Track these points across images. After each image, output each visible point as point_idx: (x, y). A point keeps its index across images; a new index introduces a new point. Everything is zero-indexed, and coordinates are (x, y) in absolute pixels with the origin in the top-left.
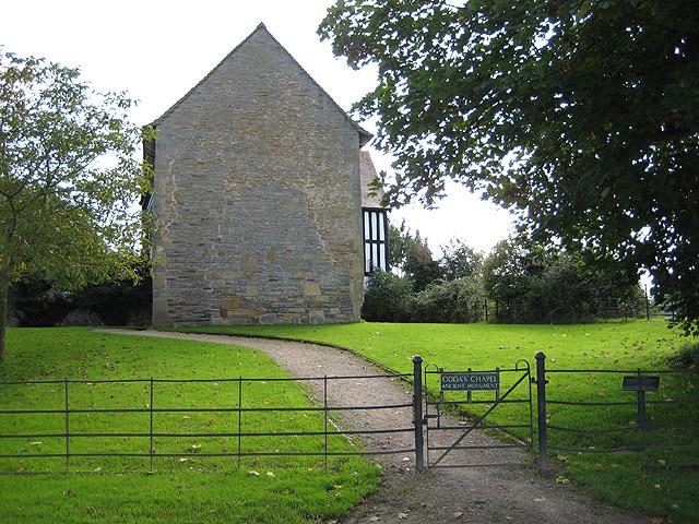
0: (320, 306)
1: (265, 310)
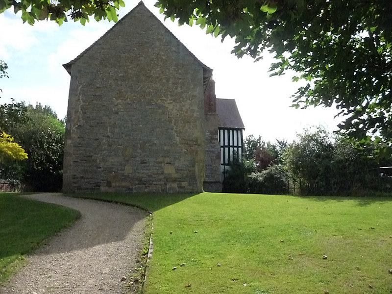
0: (174, 181)
1: (137, 182)
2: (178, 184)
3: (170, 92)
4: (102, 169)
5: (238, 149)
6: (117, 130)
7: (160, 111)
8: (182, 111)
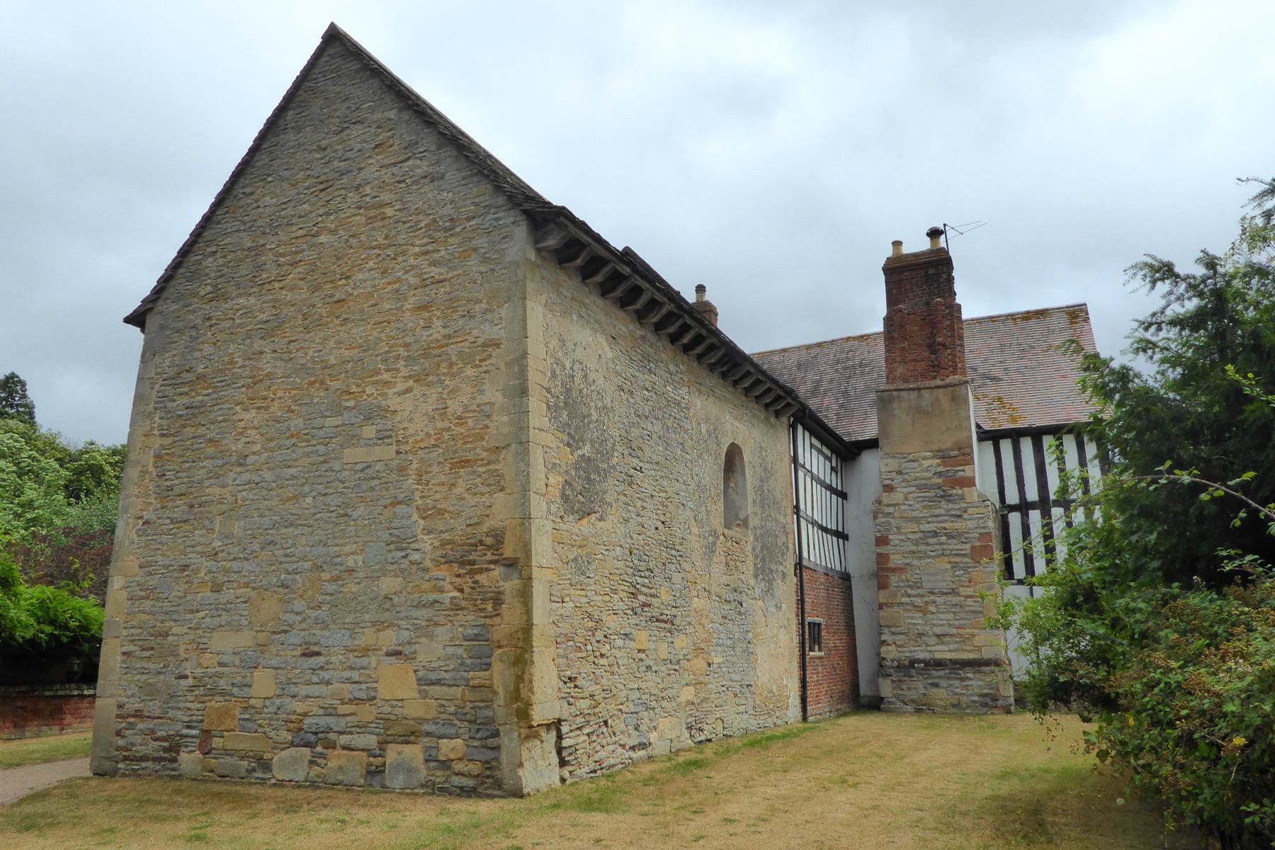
2: (427, 749)
3: (407, 345)
5: (1025, 517)
6: (238, 528)
7: (369, 431)
8: (443, 415)
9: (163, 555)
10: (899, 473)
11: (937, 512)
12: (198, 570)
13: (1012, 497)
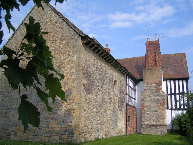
4: (12, 123)
9: (6, 99)
10: (147, 86)
11: (154, 95)
12: (13, 102)
13: (169, 92)
